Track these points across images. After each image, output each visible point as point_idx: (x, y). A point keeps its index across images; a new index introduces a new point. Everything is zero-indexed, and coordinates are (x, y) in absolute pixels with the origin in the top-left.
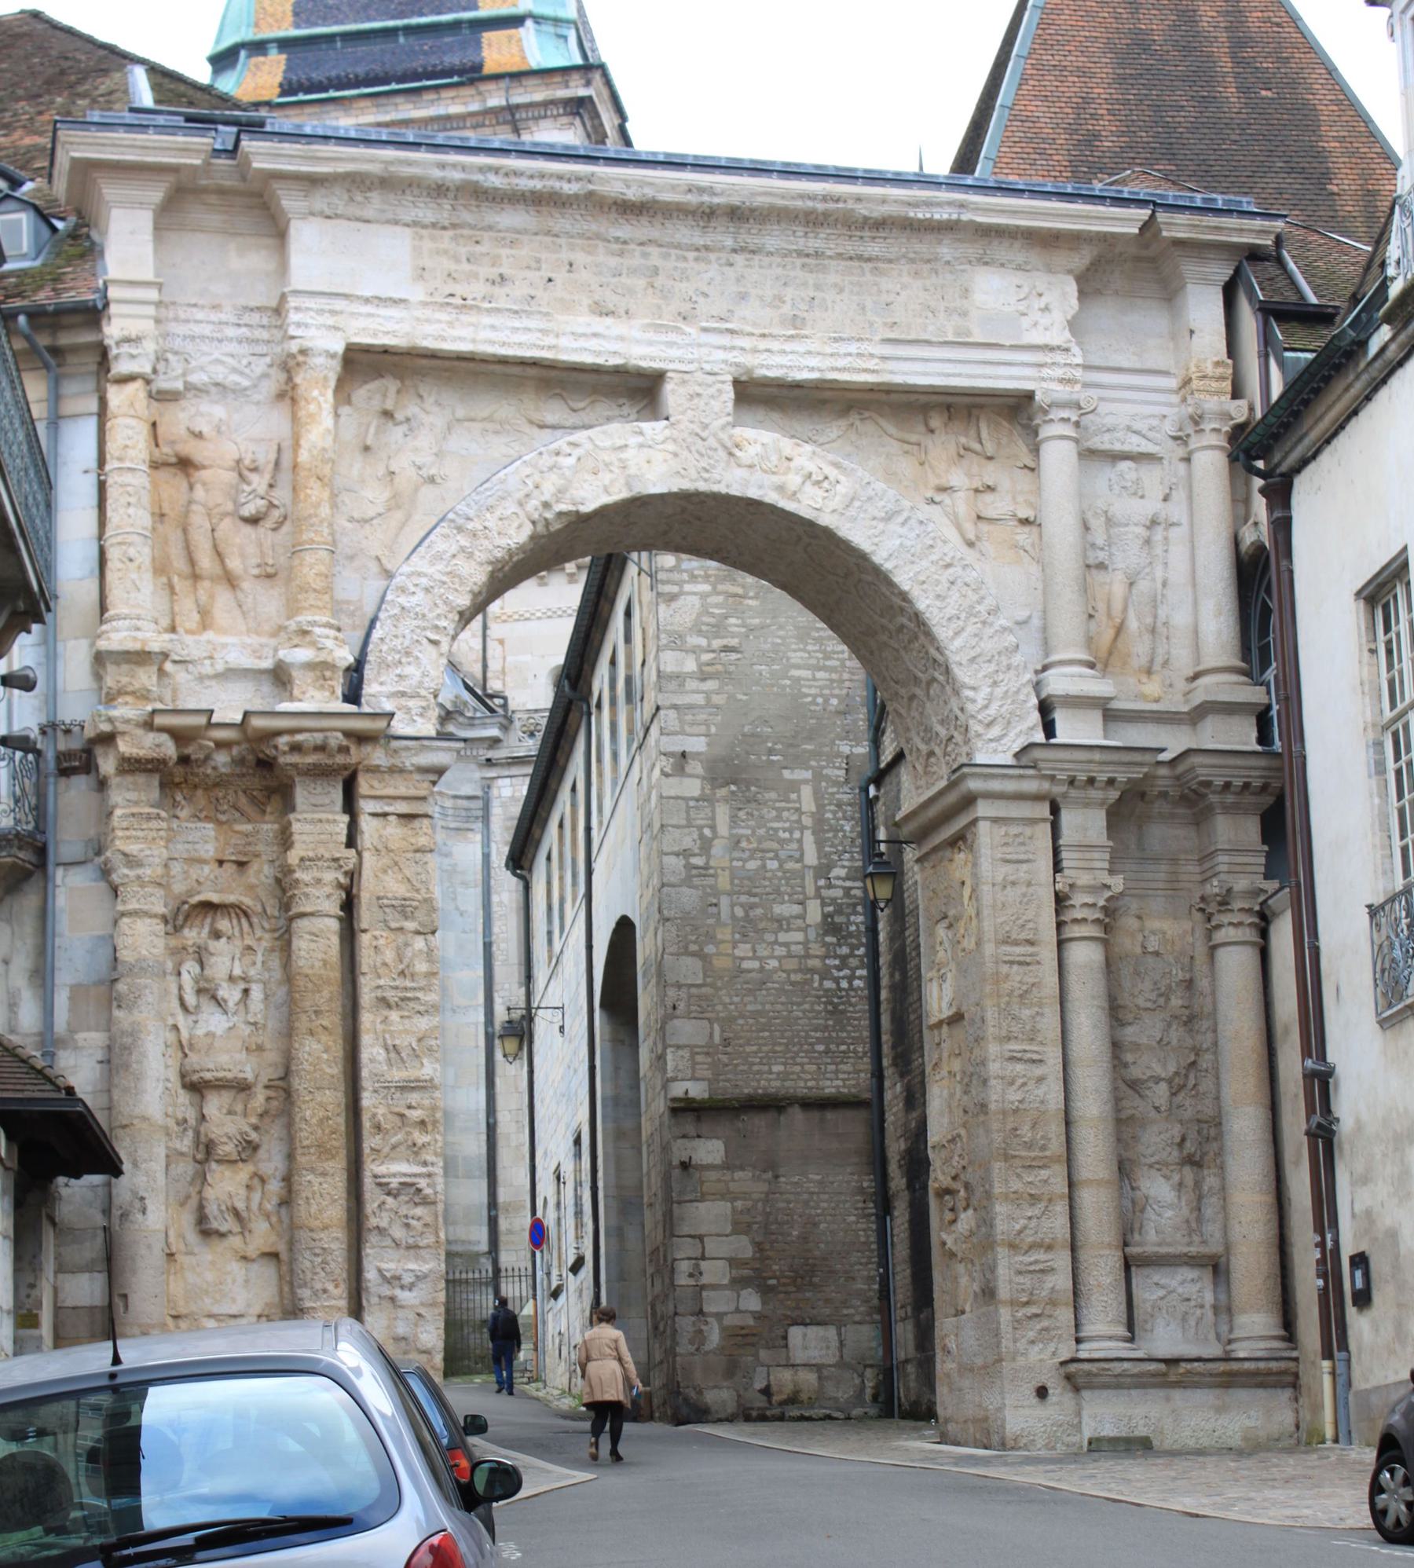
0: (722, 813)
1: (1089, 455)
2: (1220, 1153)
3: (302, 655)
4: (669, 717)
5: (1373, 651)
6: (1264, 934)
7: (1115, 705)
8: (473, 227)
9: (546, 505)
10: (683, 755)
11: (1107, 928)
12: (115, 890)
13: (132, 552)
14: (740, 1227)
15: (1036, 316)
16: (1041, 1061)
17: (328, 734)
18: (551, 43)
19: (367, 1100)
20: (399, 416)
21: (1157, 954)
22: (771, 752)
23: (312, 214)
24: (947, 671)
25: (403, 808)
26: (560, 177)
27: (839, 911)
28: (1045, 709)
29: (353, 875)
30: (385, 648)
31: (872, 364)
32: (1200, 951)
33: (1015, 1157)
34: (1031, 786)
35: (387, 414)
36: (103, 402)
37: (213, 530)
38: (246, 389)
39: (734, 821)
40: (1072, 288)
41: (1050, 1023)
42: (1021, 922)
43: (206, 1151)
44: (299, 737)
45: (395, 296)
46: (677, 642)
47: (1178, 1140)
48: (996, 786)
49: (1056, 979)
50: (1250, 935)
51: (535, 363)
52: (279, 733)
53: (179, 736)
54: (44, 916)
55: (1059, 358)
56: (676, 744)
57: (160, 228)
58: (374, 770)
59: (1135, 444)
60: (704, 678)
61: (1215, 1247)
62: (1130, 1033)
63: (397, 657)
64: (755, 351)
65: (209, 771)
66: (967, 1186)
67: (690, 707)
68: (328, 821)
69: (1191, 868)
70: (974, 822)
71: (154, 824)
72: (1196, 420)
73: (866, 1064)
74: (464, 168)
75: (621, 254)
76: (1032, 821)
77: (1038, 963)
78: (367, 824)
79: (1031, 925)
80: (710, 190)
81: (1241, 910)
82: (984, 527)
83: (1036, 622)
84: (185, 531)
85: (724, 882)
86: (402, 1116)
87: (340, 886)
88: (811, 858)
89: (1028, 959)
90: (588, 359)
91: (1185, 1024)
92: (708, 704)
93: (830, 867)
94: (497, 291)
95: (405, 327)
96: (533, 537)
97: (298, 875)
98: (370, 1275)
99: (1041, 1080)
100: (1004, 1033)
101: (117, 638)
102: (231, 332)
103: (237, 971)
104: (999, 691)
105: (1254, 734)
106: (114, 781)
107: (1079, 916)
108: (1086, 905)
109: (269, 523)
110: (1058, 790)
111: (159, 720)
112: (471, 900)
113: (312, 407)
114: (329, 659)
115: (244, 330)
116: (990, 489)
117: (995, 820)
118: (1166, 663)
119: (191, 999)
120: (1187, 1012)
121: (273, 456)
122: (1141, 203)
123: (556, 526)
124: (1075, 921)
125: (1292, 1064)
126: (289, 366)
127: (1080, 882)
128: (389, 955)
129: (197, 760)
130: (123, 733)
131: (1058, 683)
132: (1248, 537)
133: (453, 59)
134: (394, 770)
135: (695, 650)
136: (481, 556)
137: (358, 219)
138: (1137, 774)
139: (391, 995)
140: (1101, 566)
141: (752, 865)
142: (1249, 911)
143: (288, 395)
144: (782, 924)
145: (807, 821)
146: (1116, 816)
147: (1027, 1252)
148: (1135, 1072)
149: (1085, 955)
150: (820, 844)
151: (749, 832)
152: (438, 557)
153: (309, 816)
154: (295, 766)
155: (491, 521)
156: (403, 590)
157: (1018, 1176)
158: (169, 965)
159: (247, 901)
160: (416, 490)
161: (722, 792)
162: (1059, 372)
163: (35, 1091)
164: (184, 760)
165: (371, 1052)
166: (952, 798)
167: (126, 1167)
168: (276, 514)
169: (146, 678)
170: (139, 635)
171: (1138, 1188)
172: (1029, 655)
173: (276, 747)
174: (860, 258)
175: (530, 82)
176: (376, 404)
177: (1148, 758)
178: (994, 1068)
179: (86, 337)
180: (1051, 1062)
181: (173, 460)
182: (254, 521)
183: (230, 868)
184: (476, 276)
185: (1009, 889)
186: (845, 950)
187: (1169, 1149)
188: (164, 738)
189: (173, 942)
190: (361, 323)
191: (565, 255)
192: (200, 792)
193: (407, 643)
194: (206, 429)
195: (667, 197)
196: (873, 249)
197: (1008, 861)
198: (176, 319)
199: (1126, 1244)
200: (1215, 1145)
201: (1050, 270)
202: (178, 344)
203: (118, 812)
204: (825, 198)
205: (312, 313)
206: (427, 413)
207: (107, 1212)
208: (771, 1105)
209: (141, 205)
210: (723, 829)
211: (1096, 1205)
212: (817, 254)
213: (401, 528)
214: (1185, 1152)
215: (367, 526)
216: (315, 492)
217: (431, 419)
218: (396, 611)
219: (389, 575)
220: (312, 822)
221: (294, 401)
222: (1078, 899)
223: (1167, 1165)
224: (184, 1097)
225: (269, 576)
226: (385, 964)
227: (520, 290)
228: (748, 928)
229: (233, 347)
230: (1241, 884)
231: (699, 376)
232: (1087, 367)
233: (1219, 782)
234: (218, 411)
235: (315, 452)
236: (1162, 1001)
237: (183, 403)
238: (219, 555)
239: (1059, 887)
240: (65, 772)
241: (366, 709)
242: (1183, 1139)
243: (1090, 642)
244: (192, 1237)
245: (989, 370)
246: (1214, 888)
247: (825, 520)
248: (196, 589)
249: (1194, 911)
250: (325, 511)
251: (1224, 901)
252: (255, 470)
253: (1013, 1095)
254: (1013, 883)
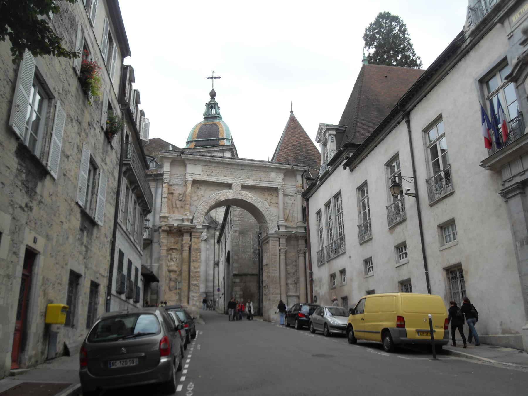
0: (241, 238)
1: (285, 195)
2: (299, 283)
3: (186, 217)
4: (234, 226)
5: (318, 220)
6: (305, 255)
7: (287, 226)
9: (217, 200)
10: (236, 230)
11: (286, 254)
12: (160, 246)
14: (241, 290)
15: (278, 178)
18: (228, 142)
19: (191, 274)
20: (199, 188)
21: (292, 257)
22: (247, 230)
24: (266, 221)
25: (197, 237)
26: (220, 160)
27: (255, 250)
28: (278, 226)
29: (191, 245)
31: (258, 184)
32: (297, 257)
34: (276, 236)
35: (198, 188)
36: (162, 186)
39: (242, 239)
40: (283, 175)
41: (278, 266)
43: (170, 279)
44: (184, 228)
46: (236, 216)
48: (272, 236)
50: (303, 255)
51: (216, 182)
52: (182, 227)
53: (170, 227)
54: (151, 249)
55: (281, 183)
56: (235, 229)
57: (171, 165)
58: (193, 232)
59: (290, 194)
60: (239, 221)
61: (298, 294)
62: (288, 267)
64: (244, 182)
66: (267, 286)
67: (237, 224)
70: (269, 240)
72: (298, 191)
73: (258, 270)
74: (208, 158)
75: (227, 169)
76: (276, 240)
78: (193, 239)
80: (238, 162)
82: (271, 204)
83: (278, 216)
85: (241, 246)
86: (195, 276)
87: (189, 246)
88: (252, 243)
90: (223, 182)
92: (239, 224)
93: (254, 245)
94: (212, 174)
95: (200, 178)
96: (215, 203)
97: (184, 245)
98: (190, 296)
99: (277, 273)
101: (162, 215)
102: (179, 178)
103: (176, 257)
104: (273, 224)
105: (304, 230)
106: (161, 233)
107: (282, 252)
109: (183, 201)
110: (280, 236)
111: (167, 225)
112: (212, 247)
116: (272, 199)
117: (272, 240)
118: (294, 221)
119: (169, 260)
121: (183, 193)
122: (291, 165)
123: (218, 202)
125: (308, 271)
126: (186, 182)
128: (195, 255)
131: (280, 223)
132: (304, 206)
133: (216, 143)
134: (196, 232)
135: (238, 217)
136: (208, 206)
138: (290, 235)
139: (195, 260)
140: (286, 209)
141: (244, 244)
143: (185, 185)
144: (248, 252)
145: (251, 239)
146: (287, 241)
148: (289, 272)
149: (283, 257)
150: (253, 242)
152: (203, 206)
155: (210, 201)
156: (199, 210)
158: (167, 256)
159: (177, 248)
160: (201, 197)
161: (241, 235)
162: (281, 185)
163: (148, 272)
164: (170, 230)
165: (192, 268)
166: (266, 237)
167: (160, 281)
168: (183, 200)
169: (166, 220)
172: (277, 219)
174: (257, 171)
175: (225, 146)
177: (291, 233)
178: (271, 271)
179: (161, 178)
182: (181, 201)
183: (175, 244)
184: (209, 172)
186: (255, 255)
189: (168, 253)
191: (221, 169)
194: (175, 189)
195: (233, 163)
196: (258, 170)
199: (287, 294)
201: (280, 173)
202: (172, 179)
203: (161, 236)
204: (253, 163)
207: (157, 287)
208: (246, 275)
210: (241, 240)
211: (283, 289)
212: (252, 170)
216: (189, 198)
219: (197, 208)
221: (186, 186)
222: (282, 250)
224: (168, 273)
226: (194, 257)
227: (215, 173)
228: (244, 252)
230: (302, 248)
231: (237, 184)
232: (284, 184)
233: (300, 236)
234: (177, 187)
238: (176, 205)
240: (155, 231)
241: (193, 224)
243: (284, 218)
244: (168, 291)
245: (272, 185)
246: (299, 249)
247: (252, 202)
250: (189, 200)
251: (300, 251)
252: (181, 194)
253: (273, 275)
254: (274, 248)
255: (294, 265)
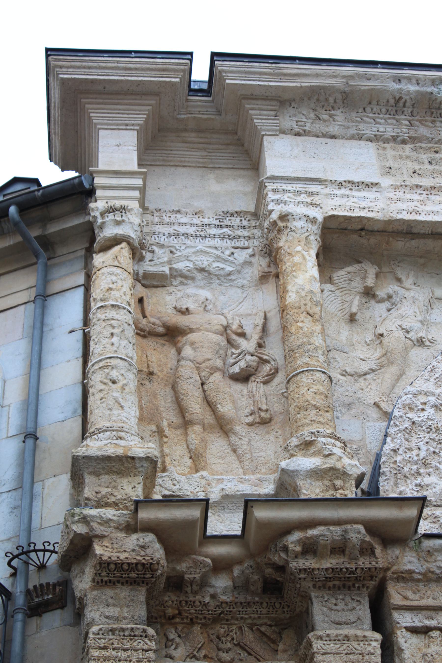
8: (430, 140)
13: (114, 374)
17: (348, 527)
20: (381, 293)
23: (283, 132)
30: (399, 459)
37: (202, 384)
38: (230, 274)
45: (368, 180)
63: (415, 467)
65: (207, 599)
68: (357, 638)
71: (139, 644)
84: (174, 387)
95: (381, 204)
102: (213, 231)
106: (89, 599)
113: (297, 259)
114: (339, 466)
115: (225, 230)
129: (192, 582)
130: (102, 537)
137: (324, 136)
153: (333, 632)
154: (309, 571)
160: (407, 350)
168: (266, 368)
170: (122, 443)
173: (285, 549)
176: (358, 285)
181: (161, 330)
188: (150, 537)
190: (337, 201)
192: (197, 629)
193: (423, 454)
194: (192, 307)
198: (161, 223)
205: (289, 195)
206: (408, 289)
209: (126, 127)
213: (397, 380)
215: (361, 380)
217: (412, 293)
218: (407, 424)
220: (337, 639)
225: (264, 422)
229: (217, 242)
234: (205, 293)
235: (303, 294)
237: (171, 289)
248: (186, 434)
250: (318, 341)
252: (243, 335)
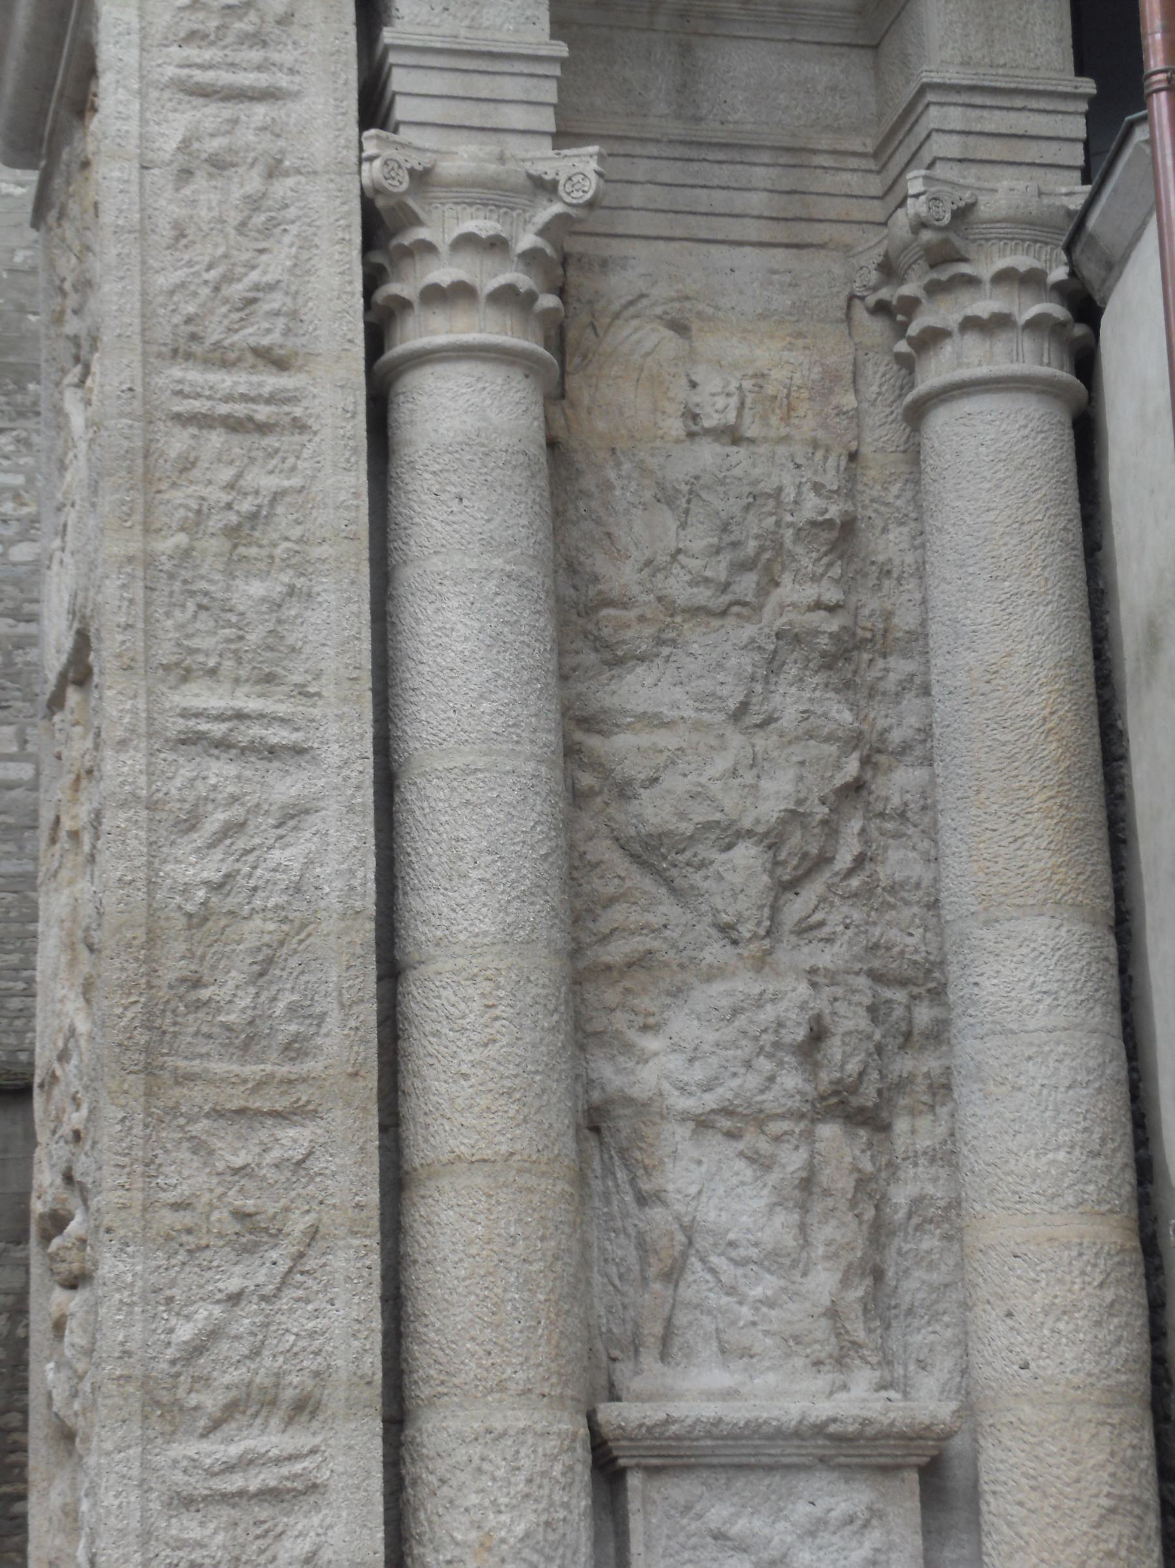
2: (942, 1088)
16: (298, 751)
21: (732, 435)
33: (184, 1079)
42: (237, 290)
47: (801, 1034)
49: (358, 479)
69: (854, 182)
77: (299, 426)
79: (275, 301)
81: (1004, 277)
89: (262, 412)
91: (829, 662)
100: (165, 652)
107: (443, 273)
108: (467, 241)
120: (834, 625)
124: (435, 295)
127: (448, 168)
142: (1031, 280)
147: (216, 1425)
151: (19, 480)
157: (199, 1147)
171: (658, 1197)
180: (333, 754)
185: (200, 181)
187: (765, 1065)
197: (205, 93)
200: (929, 1063)
214: (826, 1077)
223: (760, 1119)
236: (747, 584)
239: (372, 172)
242: (817, 1035)
249: (860, 313)
254: (219, 164)
255: (791, 638)
